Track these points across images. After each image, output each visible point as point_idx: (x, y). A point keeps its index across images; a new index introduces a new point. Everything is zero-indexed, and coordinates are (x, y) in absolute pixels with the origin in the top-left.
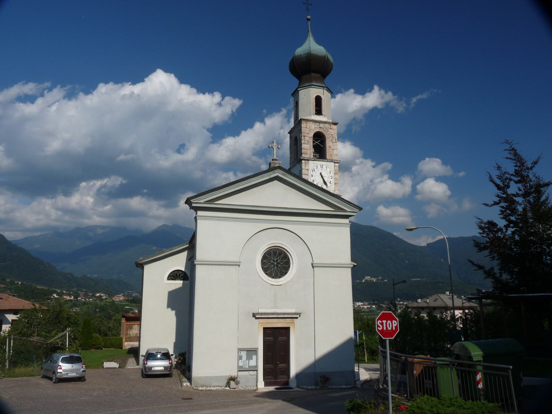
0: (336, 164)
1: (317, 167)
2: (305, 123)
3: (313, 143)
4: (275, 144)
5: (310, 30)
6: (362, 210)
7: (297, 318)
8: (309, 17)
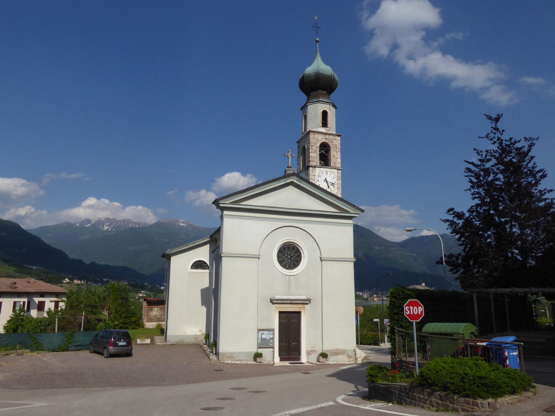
0: (339, 171)
1: (322, 173)
2: (313, 135)
3: (320, 152)
4: (290, 153)
5: (318, 51)
6: (364, 213)
7: (307, 304)
8: (318, 39)
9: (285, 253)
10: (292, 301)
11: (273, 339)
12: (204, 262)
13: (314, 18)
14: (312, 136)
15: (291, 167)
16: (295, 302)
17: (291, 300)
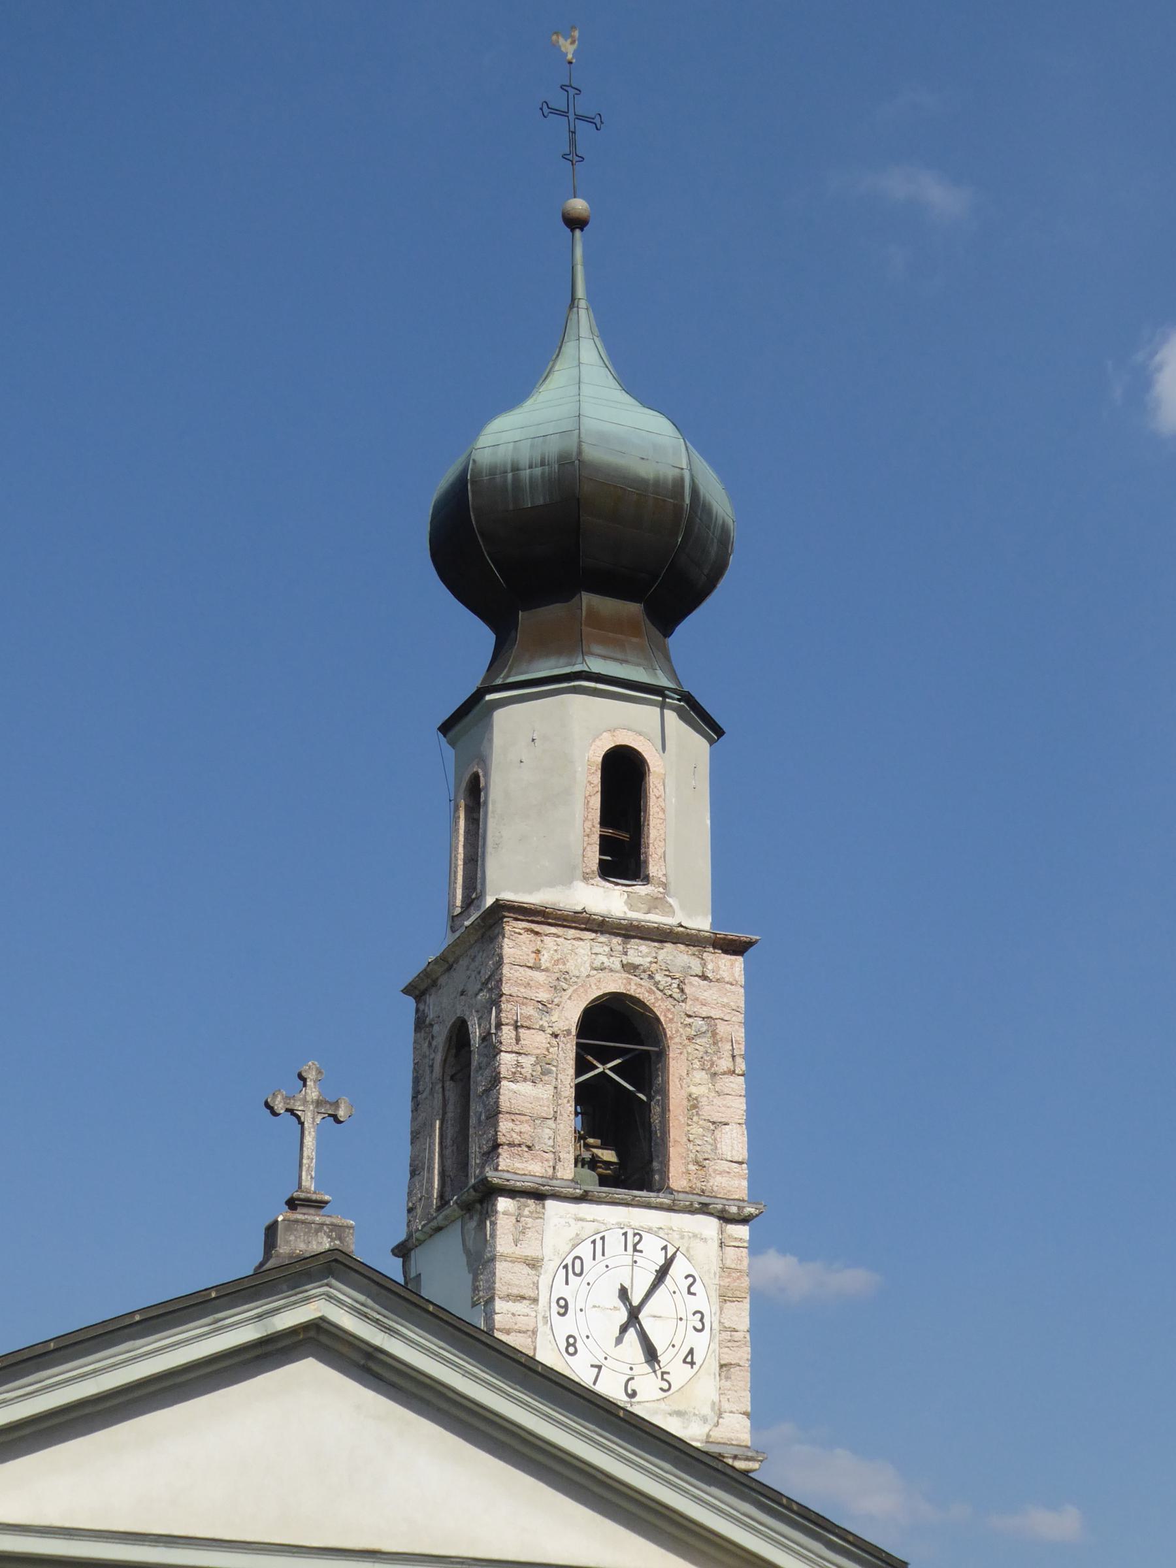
1: (599, 1243)
2: (526, 937)
3: (579, 1071)
4: (313, 1092)
5: (581, 292)
8: (579, 205)
13: (556, 46)
14: (518, 945)
15: (319, 1205)
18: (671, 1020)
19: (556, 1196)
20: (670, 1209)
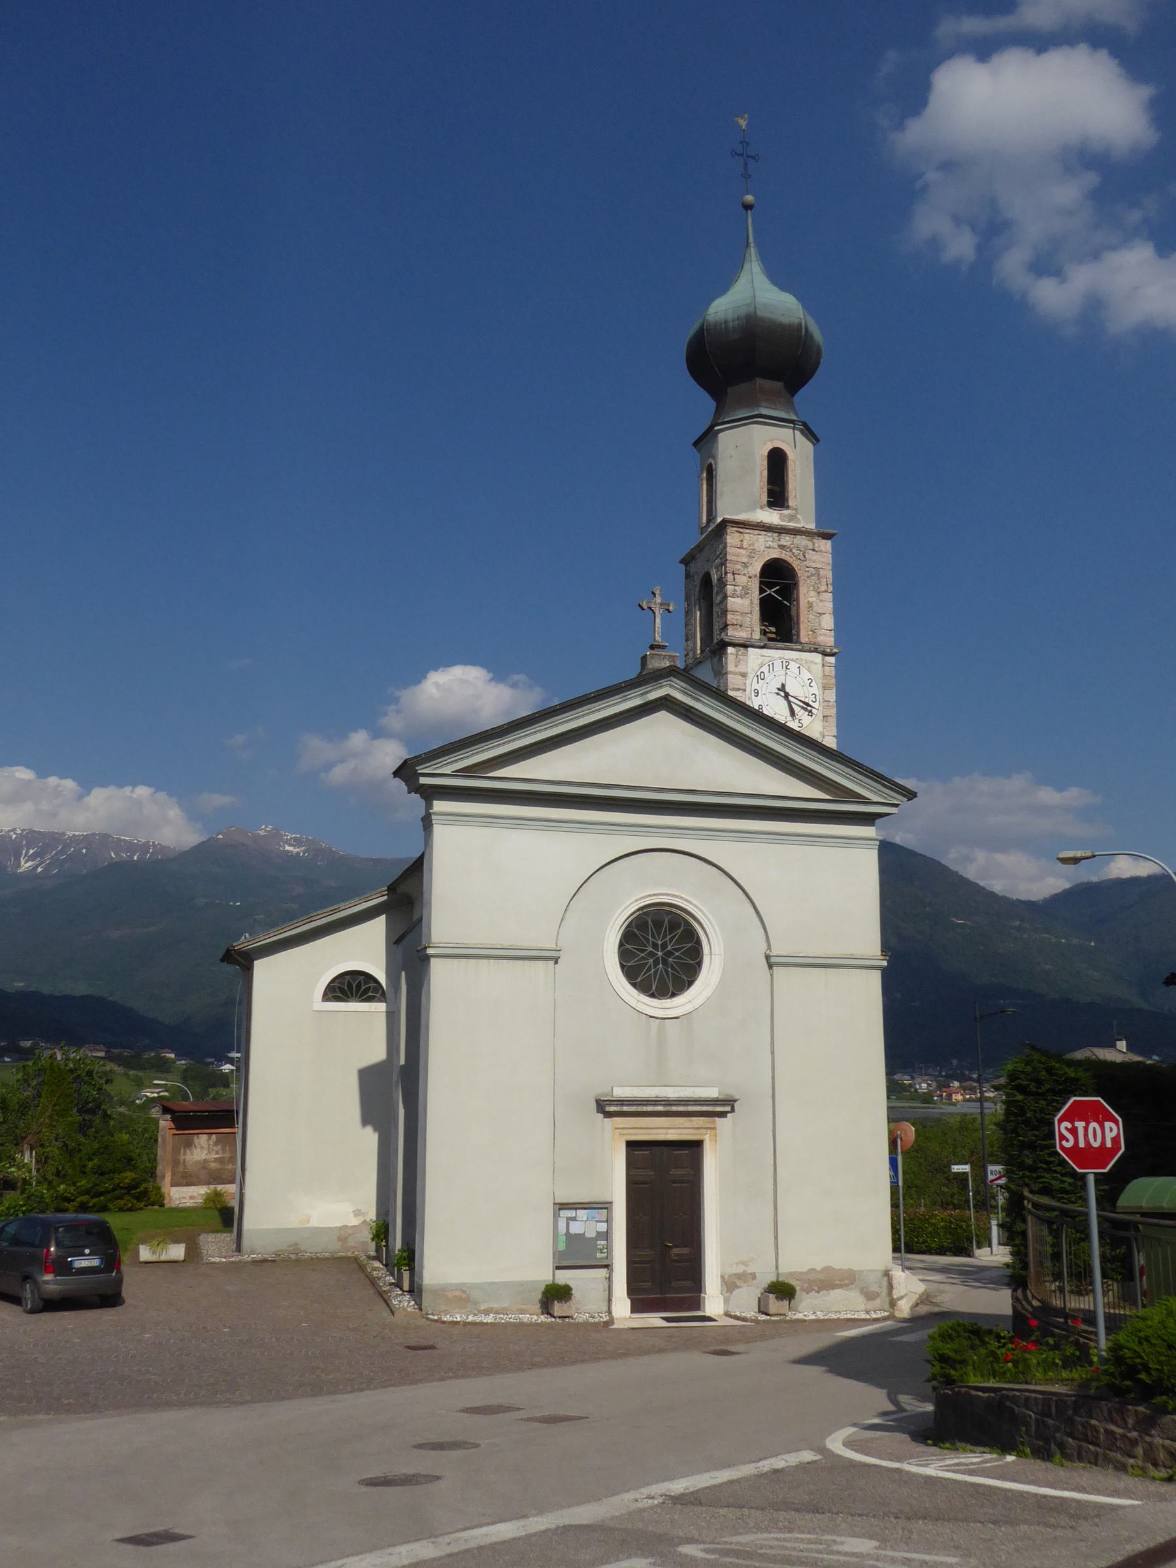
2: (737, 534)
3: (760, 594)
4: (658, 600)
5: (751, 239)
7: (723, 1115)
8: (749, 198)
9: (648, 940)
10: (671, 1105)
11: (607, 1235)
12: (369, 977)
15: (664, 647)
16: (681, 1109)
17: (668, 1102)
18: (800, 569)
19: (753, 646)
20: (801, 651)
